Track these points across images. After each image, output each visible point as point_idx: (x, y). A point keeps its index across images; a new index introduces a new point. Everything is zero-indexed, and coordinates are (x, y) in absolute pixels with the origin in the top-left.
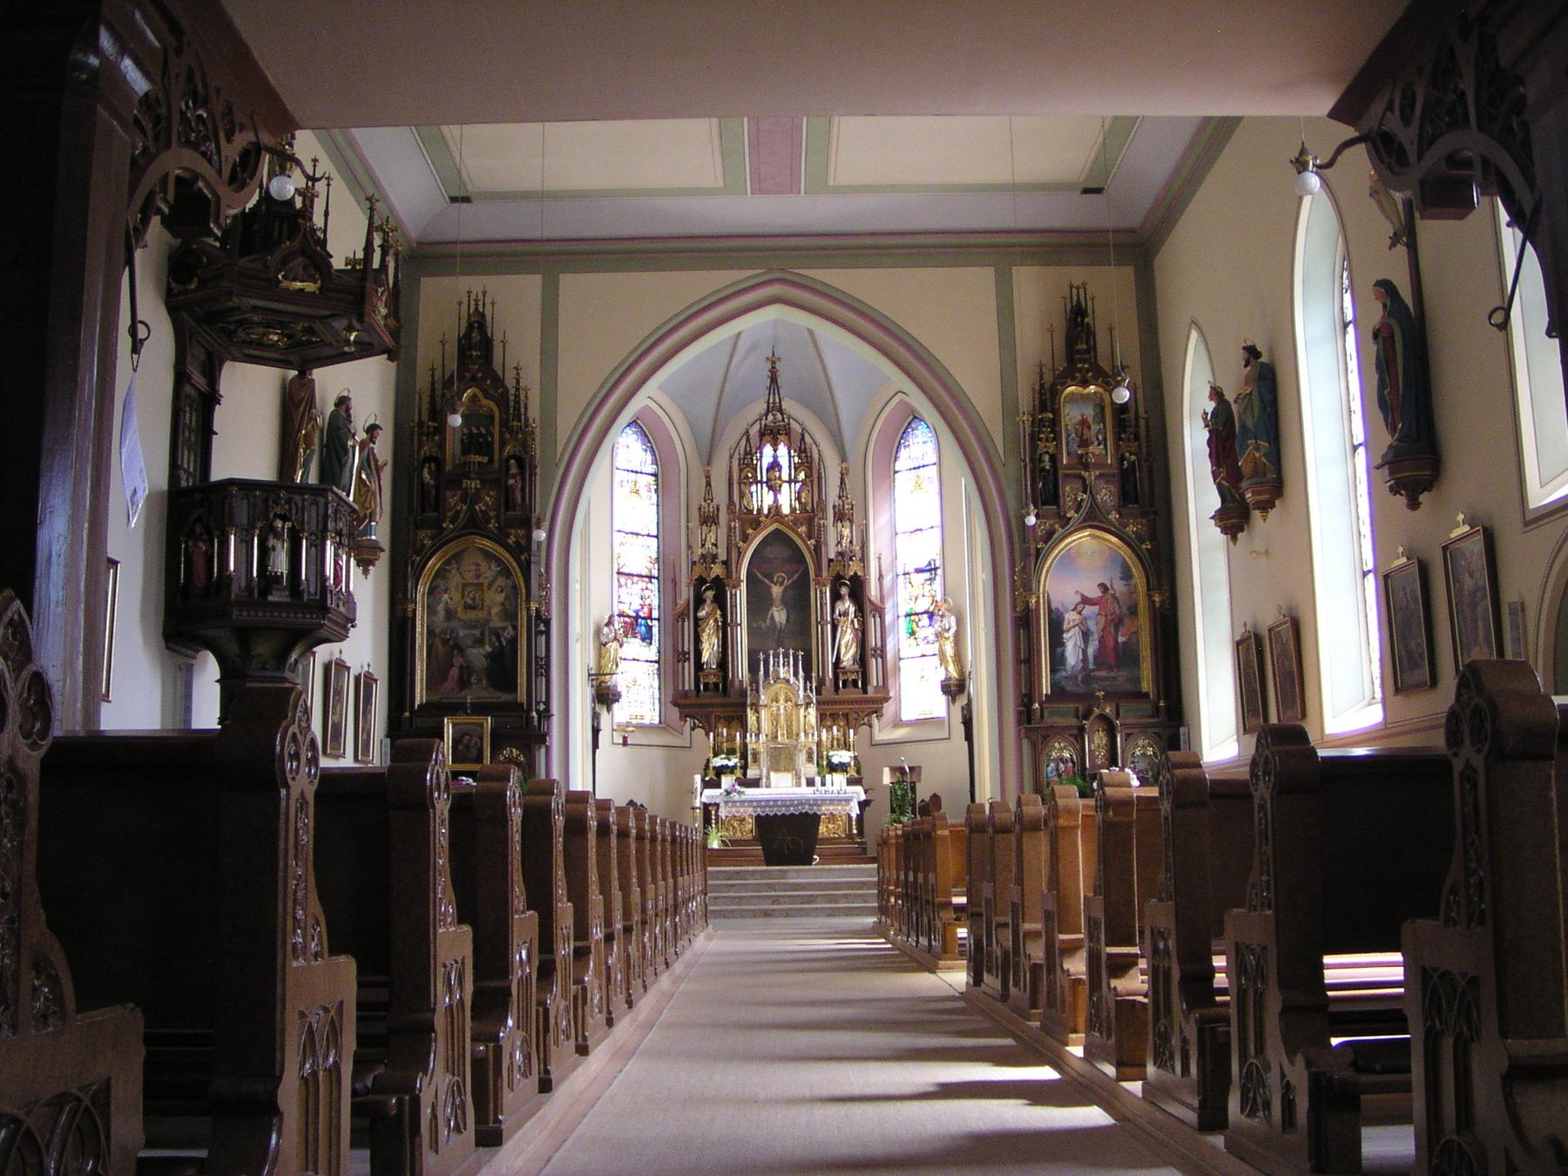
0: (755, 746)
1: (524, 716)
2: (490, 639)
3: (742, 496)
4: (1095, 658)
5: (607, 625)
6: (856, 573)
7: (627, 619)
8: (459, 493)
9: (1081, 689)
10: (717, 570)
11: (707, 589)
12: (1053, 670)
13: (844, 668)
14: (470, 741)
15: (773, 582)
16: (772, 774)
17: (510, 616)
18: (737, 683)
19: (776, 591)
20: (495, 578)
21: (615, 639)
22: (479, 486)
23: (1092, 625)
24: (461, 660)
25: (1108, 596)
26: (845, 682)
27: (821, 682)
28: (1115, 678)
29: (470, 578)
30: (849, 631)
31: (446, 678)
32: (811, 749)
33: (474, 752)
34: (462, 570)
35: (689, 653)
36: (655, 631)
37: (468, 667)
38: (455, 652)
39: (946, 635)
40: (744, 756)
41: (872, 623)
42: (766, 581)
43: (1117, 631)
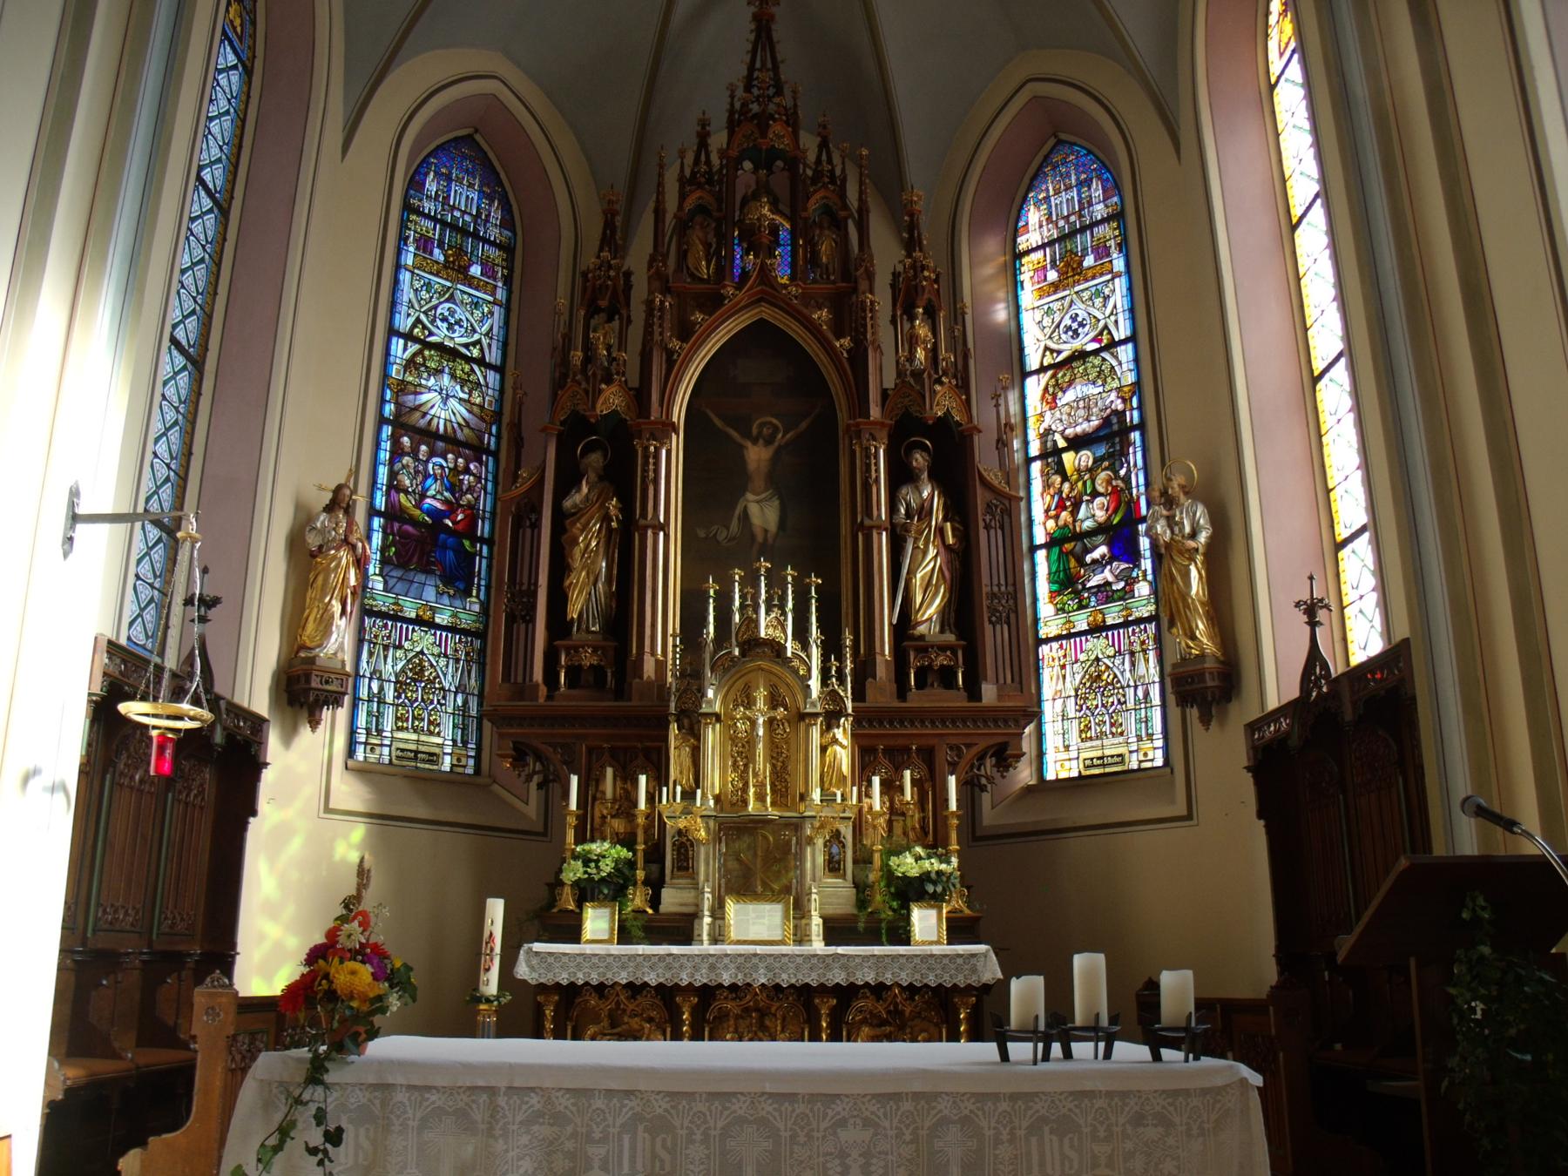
0: (682, 823)
5: (329, 508)
6: (948, 413)
10: (611, 400)
11: (588, 450)
13: (922, 637)
15: (747, 434)
16: (731, 907)
19: (757, 456)
26: (922, 674)
27: (864, 670)
32: (837, 835)
36: (481, 565)
39: (1191, 544)
40: (655, 854)
41: (988, 544)
42: (735, 434)
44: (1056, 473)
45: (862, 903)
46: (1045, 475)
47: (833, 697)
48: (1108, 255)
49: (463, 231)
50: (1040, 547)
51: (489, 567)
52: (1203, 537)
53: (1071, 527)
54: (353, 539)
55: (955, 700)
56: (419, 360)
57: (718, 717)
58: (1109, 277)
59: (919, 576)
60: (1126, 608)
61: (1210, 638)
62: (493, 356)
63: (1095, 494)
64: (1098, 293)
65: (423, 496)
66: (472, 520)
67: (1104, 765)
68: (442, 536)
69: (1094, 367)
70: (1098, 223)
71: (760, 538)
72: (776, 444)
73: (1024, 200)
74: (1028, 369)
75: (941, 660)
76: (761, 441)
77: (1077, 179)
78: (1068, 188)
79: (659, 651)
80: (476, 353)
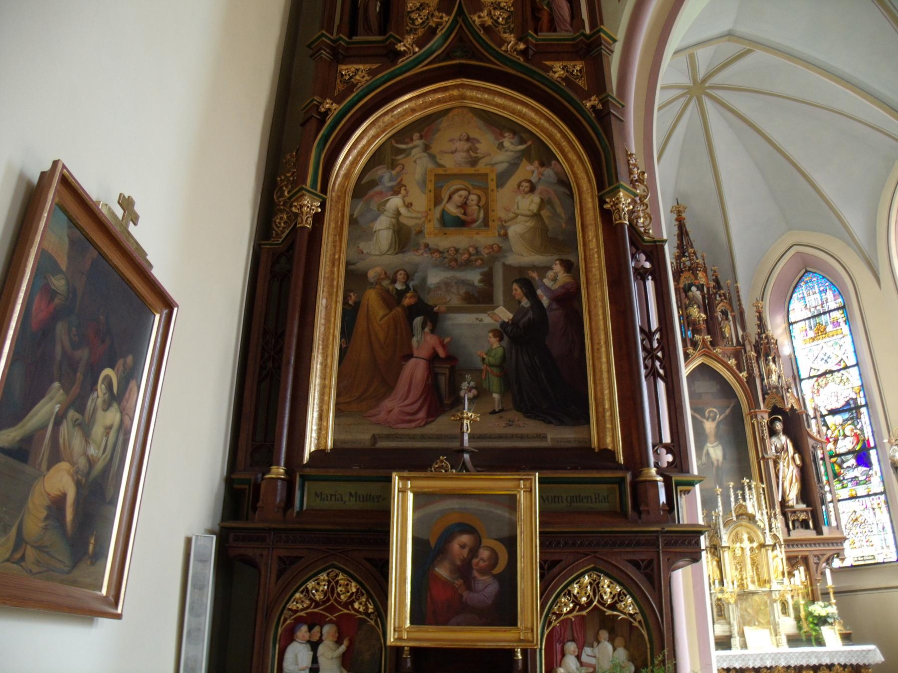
2: (508, 291)
6: (792, 406)
15: (704, 416)
20: (514, 166)
31: (389, 386)
34: (435, 150)
37: (451, 359)
38: (418, 321)
44: (823, 425)
45: (800, 628)
48: (839, 326)
53: (834, 451)
58: (841, 336)
60: (868, 488)
63: (845, 436)
64: (837, 343)
67: (864, 560)
69: (837, 377)
71: (715, 464)
72: (717, 421)
73: (791, 297)
75: (802, 517)
76: (710, 420)
77: (819, 289)
78: (814, 293)
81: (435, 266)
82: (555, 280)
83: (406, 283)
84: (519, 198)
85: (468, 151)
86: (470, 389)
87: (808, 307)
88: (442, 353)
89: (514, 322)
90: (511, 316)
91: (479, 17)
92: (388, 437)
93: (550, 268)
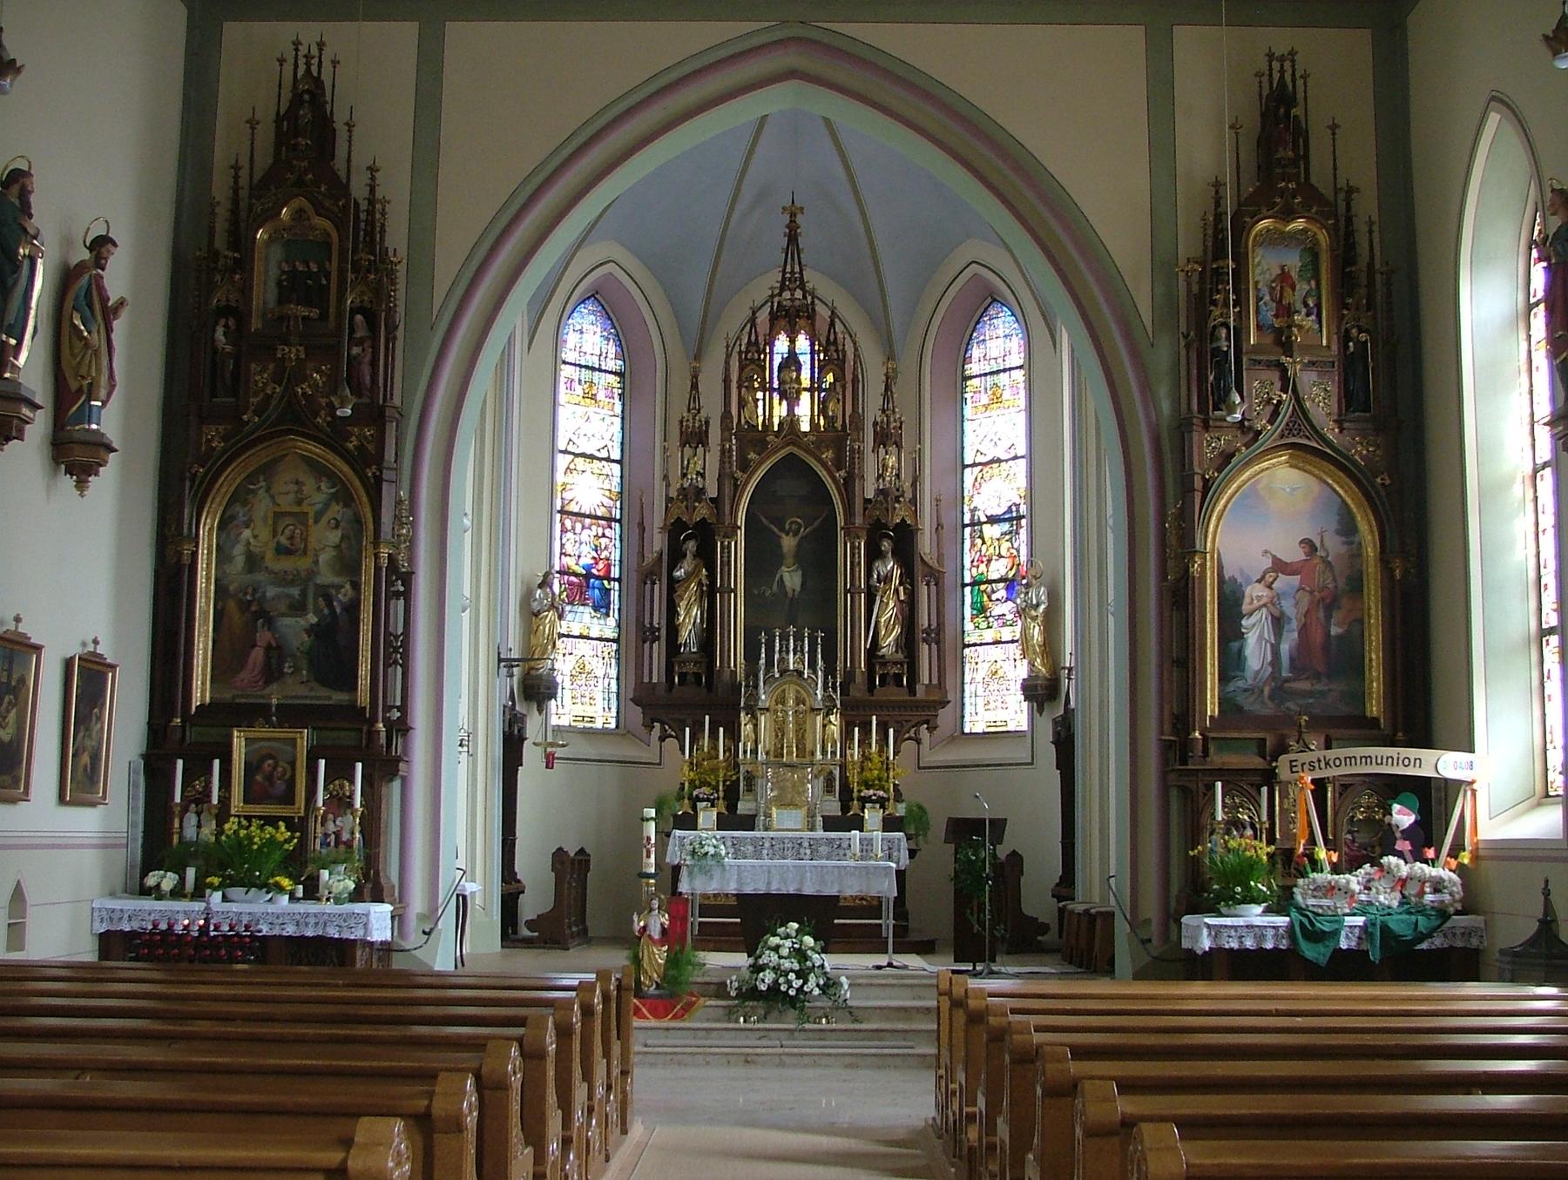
1: (365, 728)
2: (315, 600)
3: (742, 404)
4: (1292, 659)
5: (540, 586)
6: (903, 520)
7: (573, 579)
8: (271, 366)
9: (1268, 709)
10: (702, 511)
12: (1224, 678)
13: (883, 656)
14: (275, 768)
15: (782, 529)
17: (349, 566)
18: (727, 675)
19: (788, 543)
20: (327, 506)
21: (552, 606)
22: (303, 356)
23: (1288, 607)
24: (268, 635)
25: (1316, 561)
28: (1322, 693)
29: (286, 503)
30: (891, 604)
31: (242, 666)
32: (831, 773)
33: (280, 786)
35: (659, 630)
36: (615, 596)
37: (279, 647)
39: (1034, 613)
42: (775, 530)
43: (1328, 617)
46: (972, 537)
47: (828, 698)
49: (593, 369)
50: (967, 585)
51: (619, 596)
52: (1042, 607)
54: (556, 605)
55: (900, 695)
56: (572, 466)
57: (767, 710)
59: (883, 620)
61: (1043, 665)
62: (616, 455)
63: (1000, 556)
65: (579, 557)
66: (608, 567)
68: (592, 580)
70: (1013, 369)
71: (790, 594)
72: (800, 535)
74: (966, 463)
79: (732, 665)
80: (604, 454)
81: (273, 583)
82: (345, 595)
83: (253, 595)
84: (328, 533)
85: (296, 492)
86: (290, 667)
87: (988, 357)
88: (274, 645)
89: (318, 625)
90: (316, 620)
91: (302, 388)
92: (242, 696)
93: (342, 587)
